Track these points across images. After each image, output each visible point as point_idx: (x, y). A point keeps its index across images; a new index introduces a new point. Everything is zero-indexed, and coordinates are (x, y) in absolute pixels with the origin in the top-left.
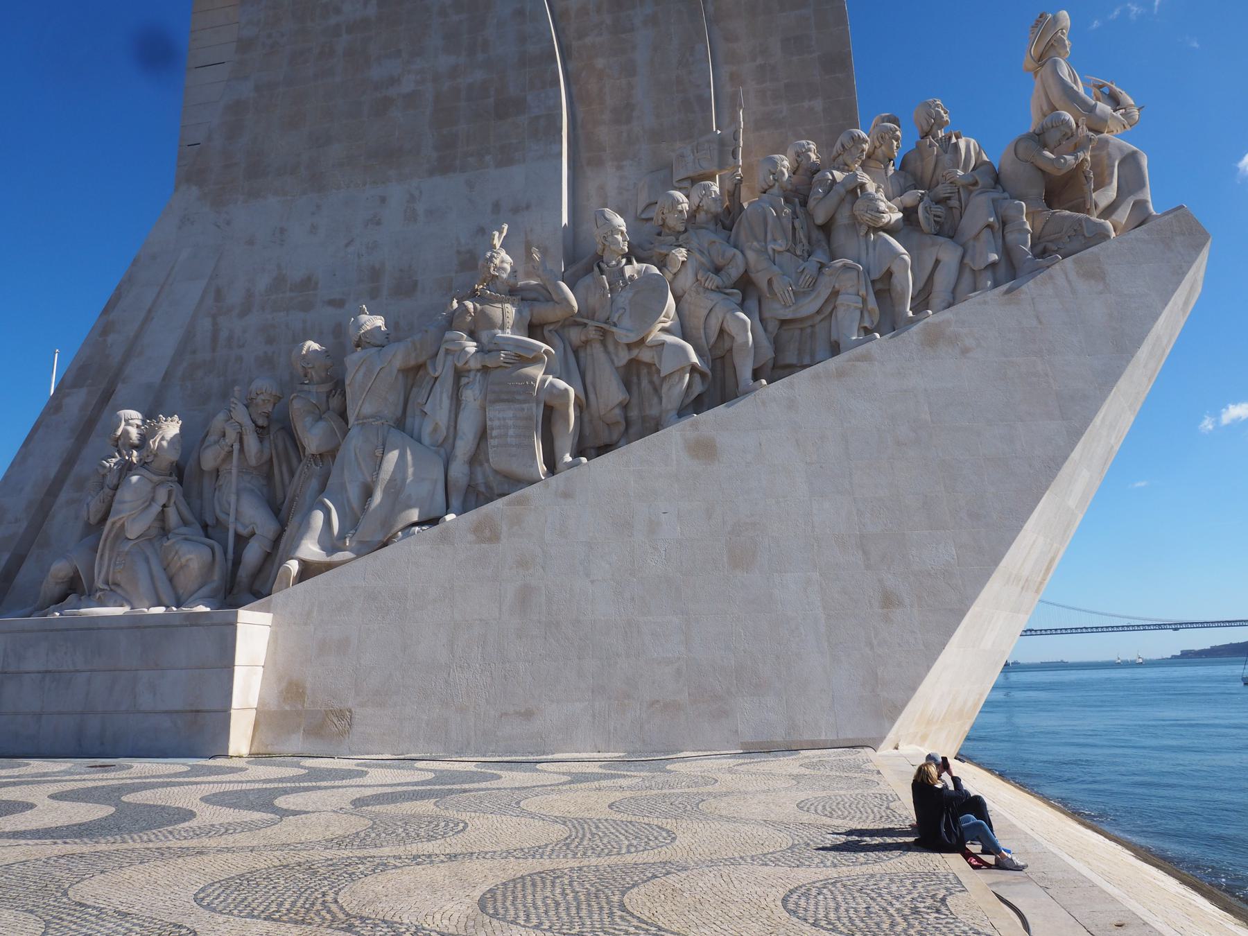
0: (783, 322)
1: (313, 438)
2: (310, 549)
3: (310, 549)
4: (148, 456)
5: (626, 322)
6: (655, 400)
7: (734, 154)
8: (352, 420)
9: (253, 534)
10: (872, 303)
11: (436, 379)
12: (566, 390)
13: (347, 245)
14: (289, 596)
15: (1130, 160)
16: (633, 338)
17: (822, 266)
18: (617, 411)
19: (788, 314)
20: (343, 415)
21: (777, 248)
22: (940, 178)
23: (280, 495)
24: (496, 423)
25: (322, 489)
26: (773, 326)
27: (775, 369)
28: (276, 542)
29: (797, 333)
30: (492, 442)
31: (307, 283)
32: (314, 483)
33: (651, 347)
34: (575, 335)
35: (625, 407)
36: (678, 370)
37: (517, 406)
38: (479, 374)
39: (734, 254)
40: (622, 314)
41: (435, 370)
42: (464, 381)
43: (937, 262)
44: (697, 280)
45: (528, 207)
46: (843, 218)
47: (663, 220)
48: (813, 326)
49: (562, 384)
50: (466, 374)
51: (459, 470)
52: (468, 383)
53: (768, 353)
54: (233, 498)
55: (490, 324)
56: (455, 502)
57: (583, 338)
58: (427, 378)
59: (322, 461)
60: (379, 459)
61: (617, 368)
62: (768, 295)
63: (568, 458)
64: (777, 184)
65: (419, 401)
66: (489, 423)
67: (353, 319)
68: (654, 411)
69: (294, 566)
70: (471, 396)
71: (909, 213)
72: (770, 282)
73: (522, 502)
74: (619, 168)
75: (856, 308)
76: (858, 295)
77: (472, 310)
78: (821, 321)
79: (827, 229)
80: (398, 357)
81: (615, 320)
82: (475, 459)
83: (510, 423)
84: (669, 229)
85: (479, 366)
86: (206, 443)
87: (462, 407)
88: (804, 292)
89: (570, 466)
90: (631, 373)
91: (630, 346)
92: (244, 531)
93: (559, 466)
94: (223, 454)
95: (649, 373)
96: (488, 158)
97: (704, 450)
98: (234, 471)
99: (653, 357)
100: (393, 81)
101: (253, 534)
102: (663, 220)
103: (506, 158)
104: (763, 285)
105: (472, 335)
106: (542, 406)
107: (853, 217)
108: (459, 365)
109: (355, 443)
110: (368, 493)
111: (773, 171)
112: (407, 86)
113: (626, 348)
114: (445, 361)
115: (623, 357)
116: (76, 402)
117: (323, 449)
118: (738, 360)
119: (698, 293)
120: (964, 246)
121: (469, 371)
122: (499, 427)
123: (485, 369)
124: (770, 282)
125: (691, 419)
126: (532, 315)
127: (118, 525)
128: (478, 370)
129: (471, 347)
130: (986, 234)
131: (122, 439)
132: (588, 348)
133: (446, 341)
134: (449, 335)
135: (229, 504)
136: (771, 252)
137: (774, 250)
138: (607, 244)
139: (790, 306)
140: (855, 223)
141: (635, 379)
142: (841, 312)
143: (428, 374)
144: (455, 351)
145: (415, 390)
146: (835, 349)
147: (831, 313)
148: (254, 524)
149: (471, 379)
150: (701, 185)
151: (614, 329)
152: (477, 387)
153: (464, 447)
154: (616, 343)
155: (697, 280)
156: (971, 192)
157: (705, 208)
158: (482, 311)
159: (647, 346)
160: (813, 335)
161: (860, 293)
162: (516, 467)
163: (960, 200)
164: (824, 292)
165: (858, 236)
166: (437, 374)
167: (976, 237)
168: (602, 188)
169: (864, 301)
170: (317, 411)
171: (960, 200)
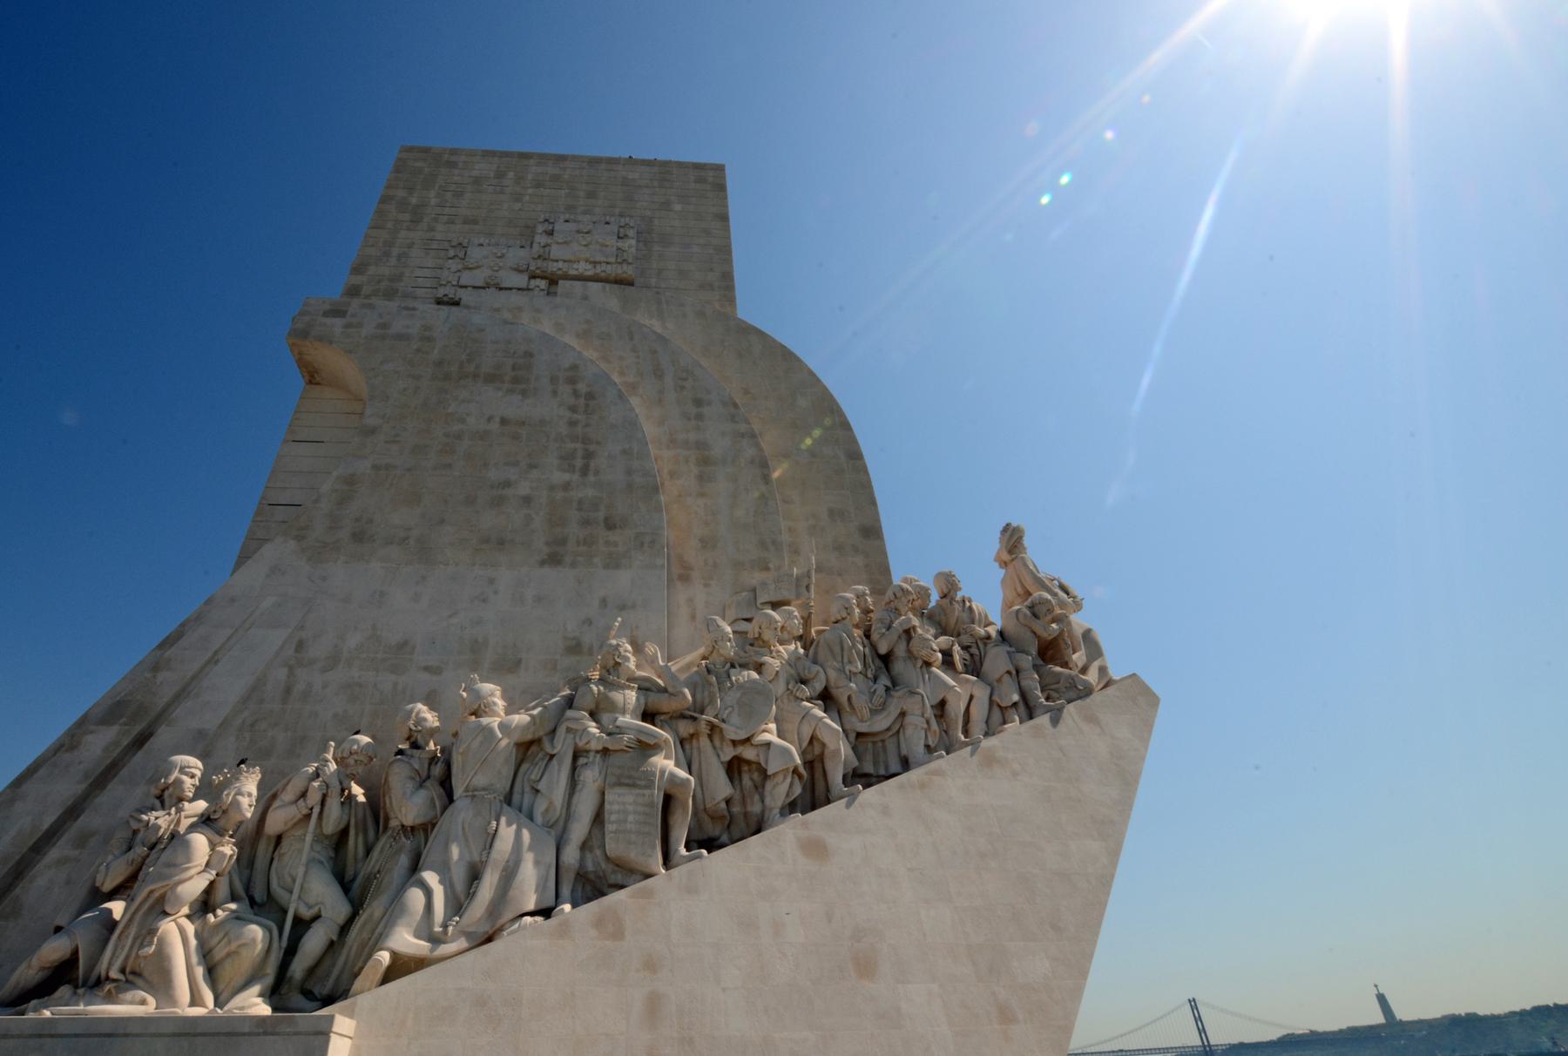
2: (405, 940)
3: (406, 939)
4: (215, 812)
5: (735, 719)
6: (757, 797)
7: (808, 587)
9: (317, 917)
11: (552, 756)
12: (688, 780)
13: (450, 616)
14: (370, 998)
15: (1087, 635)
16: (742, 735)
17: (887, 689)
18: (723, 805)
19: (863, 728)
20: (446, 783)
21: (854, 670)
22: (962, 631)
23: (350, 873)
24: (616, 807)
25: (415, 867)
26: (852, 736)
27: (861, 778)
28: (345, 929)
29: (870, 745)
30: (609, 827)
32: (404, 861)
33: (757, 746)
36: (783, 770)
37: (638, 791)
38: (598, 756)
39: (818, 672)
40: (730, 713)
41: (553, 747)
42: (582, 761)
44: (788, 689)
45: (633, 606)
46: (901, 651)
47: (760, 634)
48: (883, 741)
49: (683, 774)
50: (585, 754)
51: (571, 855)
52: (586, 764)
54: (301, 870)
55: (613, 708)
56: (566, 891)
57: (692, 731)
58: (540, 755)
59: (413, 835)
60: (490, 837)
61: (722, 763)
62: (848, 709)
63: (683, 851)
64: (849, 617)
65: (533, 777)
66: (607, 806)
67: (463, 685)
68: (755, 808)
69: (384, 957)
71: (947, 654)
72: (849, 698)
73: (648, 894)
74: (706, 585)
75: (922, 728)
76: (923, 716)
77: (596, 692)
78: (891, 736)
79: (886, 660)
81: (725, 716)
82: (585, 846)
83: (630, 808)
84: (764, 642)
85: (600, 748)
86: (277, 804)
87: (579, 787)
88: (875, 710)
89: (690, 859)
90: (734, 768)
91: (734, 743)
92: (306, 913)
93: (674, 859)
94: (299, 816)
95: (750, 770)
96: (596, 560)
97: (816, 849)
98: (309, 838)
99: (758, 755)
100: (507, 484)
101: (317, 917)
102: (760, 634)
104: (844, 700)
105: (593, 715)
106: (662, 793)
107: (909, 651)
108: (581, 744)
110: (475, 876)
111: (847, 606)
112: (524, 489)
113: (729, 743)
114: (565, 739)
115: (728, 753)
117: (419, 821)
118: (829, 765)
119: (789, 701)
121: (588, 751)
122: (618, 812)
124: (849, 698)
125: (797, 819)
126: (646, 704)
127: (157, 894)
128: (597, 752)
129: (593, 728)
130: (1007, 678)
131: (171, 789)
132: (694, 741)
133: (568, 719)
134: (570, 713)
135: (294, 881)
136: (848, 673)
137: (850, 671)
138: (716, 647)
139: (866, 721)
140: (911, 656)
141: (736, 775)
142: (909, 731)
143: (542, 749)
144: (577, 730)
145: (524, 767)
146: (906, 765)
147: (898, 732)
148: (322, 903)
149: (591, 760)
150: (785, 610)
151: (723, 726)
152: (597, 769)
153: (579, 830)
154: (722, 738)
155: (788, 689)
156: (985, 644)
157: (788, 629)
158: (604, 694)
159: (752, 745)
160: (884, 748)
161: (925, 715)
162: (633, 855)
163: (979, 649)
164: (893, 711)
165: (915, 666)
166: (555, 752)
167: (999, 680)
168: (690, 600)
169: (928, 722)
170: (418, 779)
171: (979, 649)
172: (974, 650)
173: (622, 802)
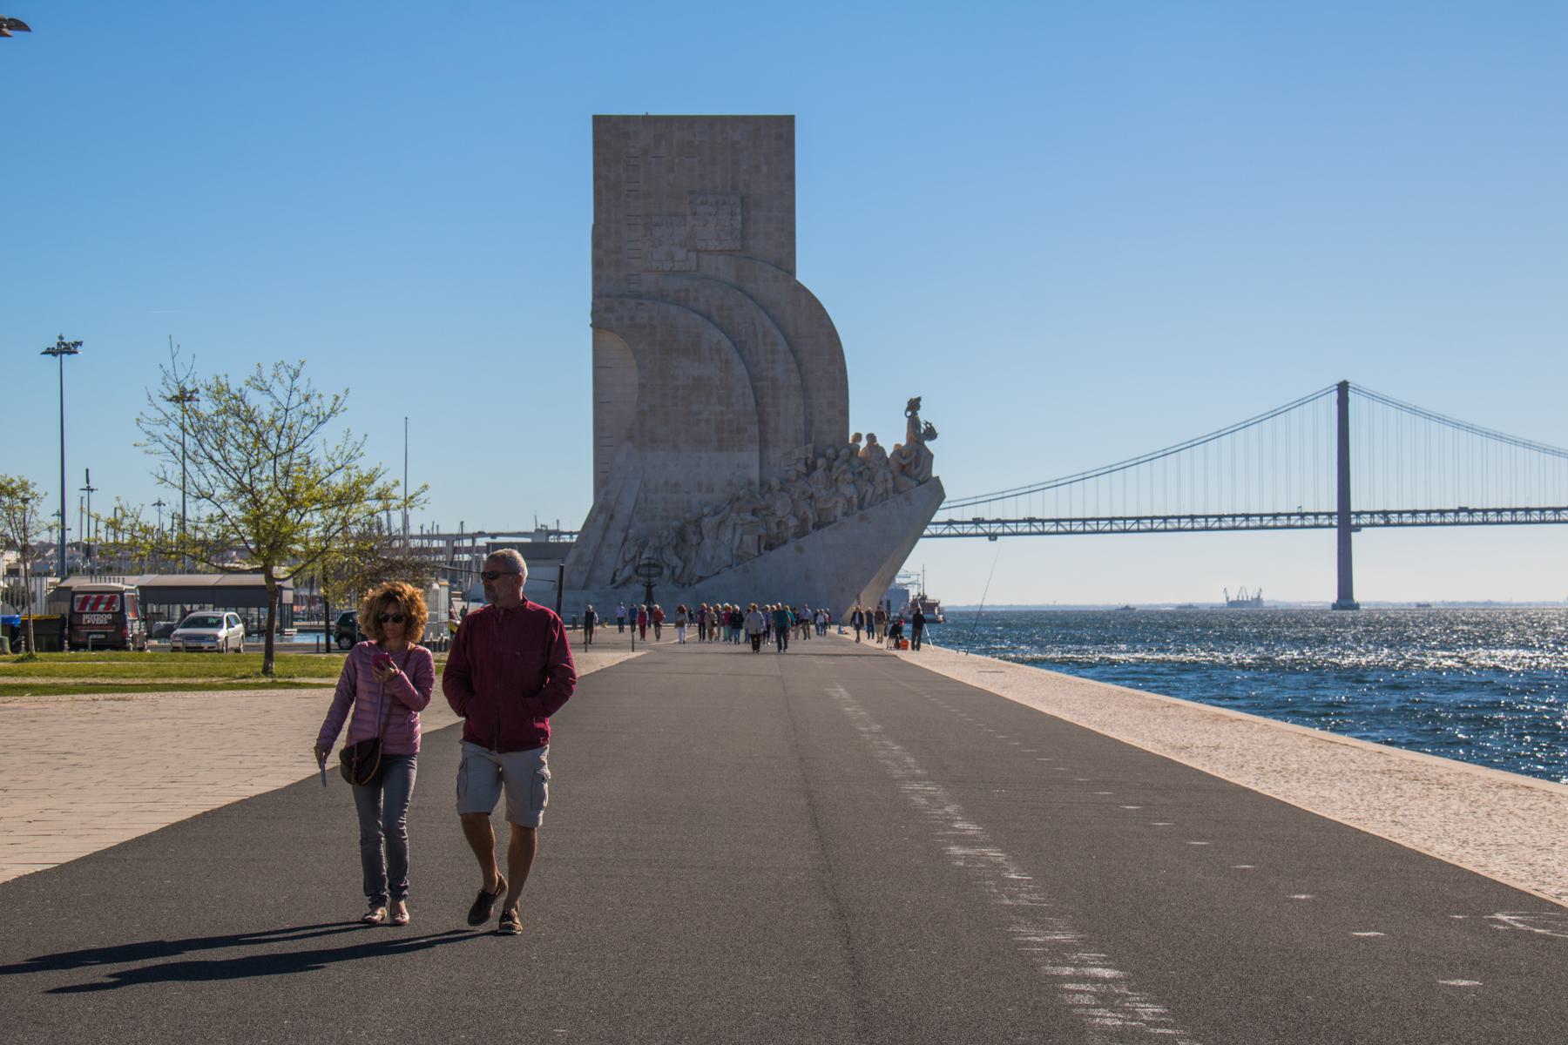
0: (822, 509)
1: (694, 539)
8: (705, 536)
9: (676, 566)
10: (846, 506)
19: (823, 506)
27: (817, 526)
28: (684, 567)
31: (676, 485)
32: (694, 554)
34: (764, 512)
35: (777, 534)
43: (867, 491)
46: (841, 478)
53: (817, 519)
70: (739, 531)
79: (836, 480)
80: (717, 518)
82: (738, 549)
101: (676, 566)
103: (741, 450)
109: (707, 541)
115: (777, 520)
116: (602, 518)
120: (873, 485)
123: (742, 525)
172: (874, 470)
173: (747, 538)
